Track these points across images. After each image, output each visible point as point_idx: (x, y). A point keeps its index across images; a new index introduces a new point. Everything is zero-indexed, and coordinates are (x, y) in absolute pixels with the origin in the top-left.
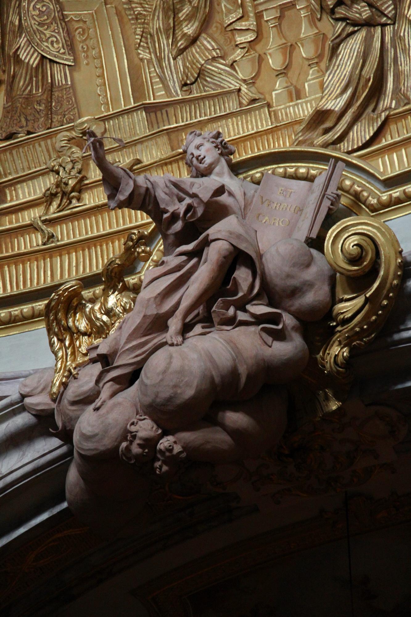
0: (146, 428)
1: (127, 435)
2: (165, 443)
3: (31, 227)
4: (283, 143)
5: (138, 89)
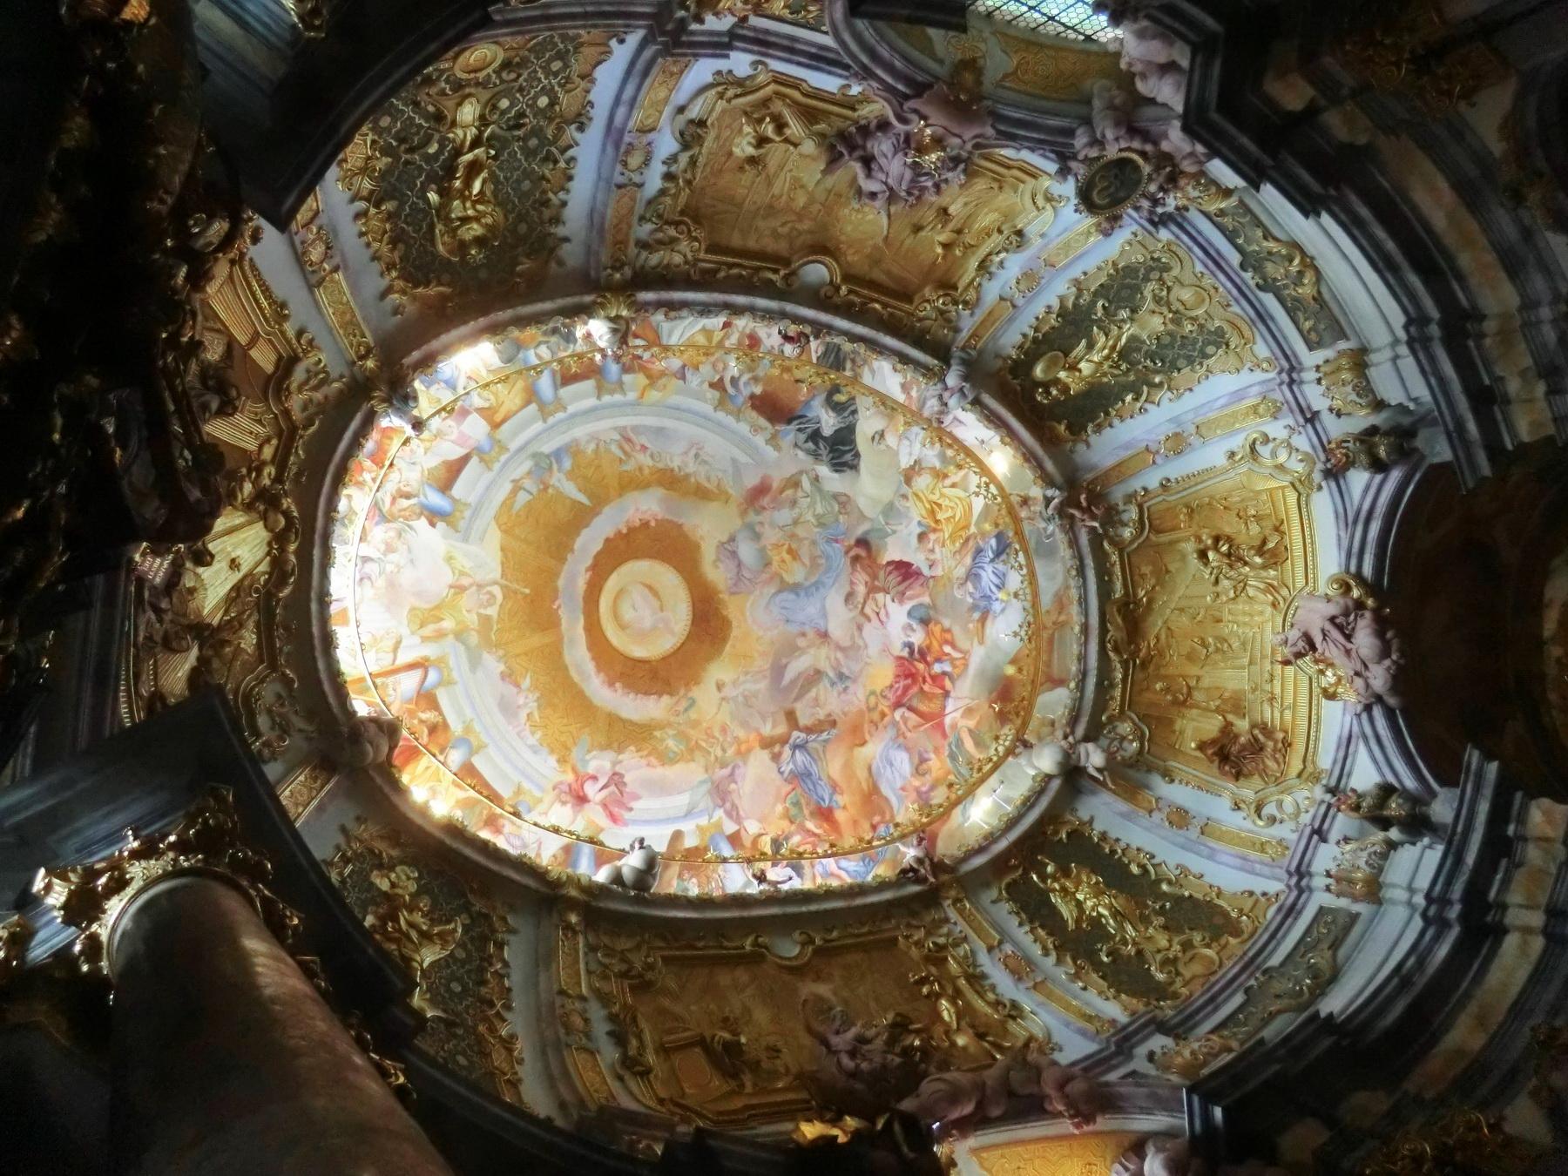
0: (1387, 662)
1: (1388, 669)
2: (1394, 657)
3: (1282, 713)
4: (1279, 620)
5: (1243, 668)
